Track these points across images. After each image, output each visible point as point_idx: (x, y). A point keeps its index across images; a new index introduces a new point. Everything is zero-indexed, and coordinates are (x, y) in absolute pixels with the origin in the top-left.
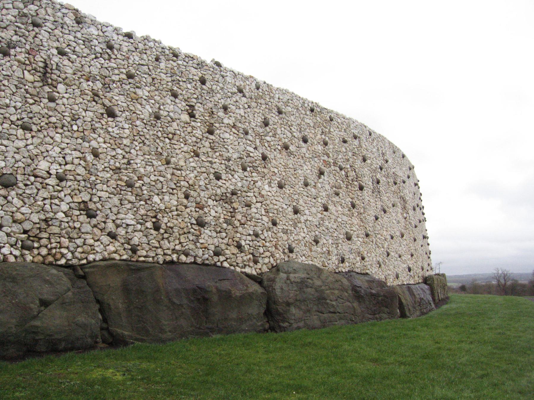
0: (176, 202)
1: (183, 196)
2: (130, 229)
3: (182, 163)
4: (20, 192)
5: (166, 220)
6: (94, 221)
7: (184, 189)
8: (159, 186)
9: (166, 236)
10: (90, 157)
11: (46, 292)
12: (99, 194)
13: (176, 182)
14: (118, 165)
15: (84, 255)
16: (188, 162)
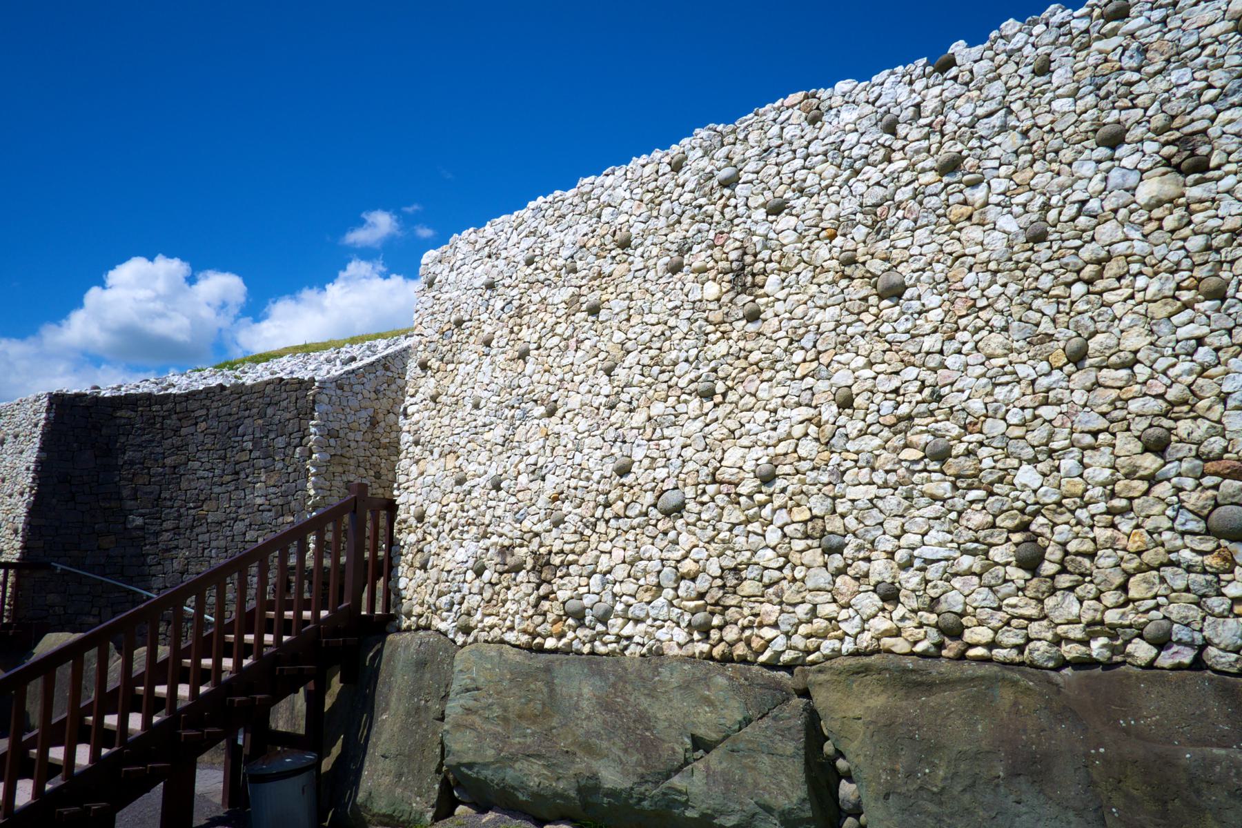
0: (1108, 472)
1: (1139, 447)
2: (933, 572)
3: (1135, 340)
4: (692, 519)
5: (1062, 533)
6: (836, 561)
7: (1139, 425)
8: (1038, 436)
9: (1064, 581)
10: (829, 412)
11: (706, 722)
12: (852, 493)
13: (1104, 409)
14: (904, 409)
15: (812, 643)
16: (1164, 329)
